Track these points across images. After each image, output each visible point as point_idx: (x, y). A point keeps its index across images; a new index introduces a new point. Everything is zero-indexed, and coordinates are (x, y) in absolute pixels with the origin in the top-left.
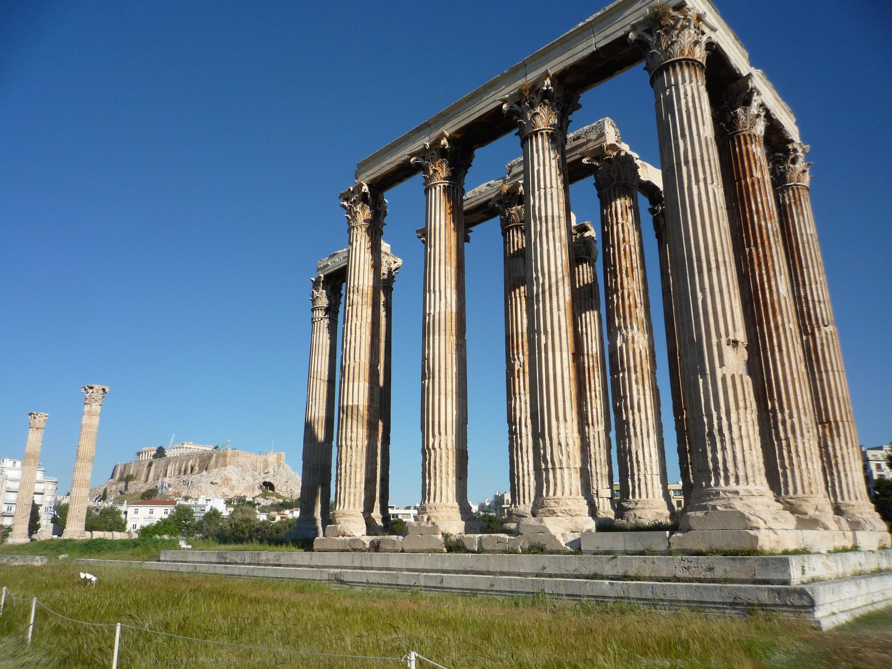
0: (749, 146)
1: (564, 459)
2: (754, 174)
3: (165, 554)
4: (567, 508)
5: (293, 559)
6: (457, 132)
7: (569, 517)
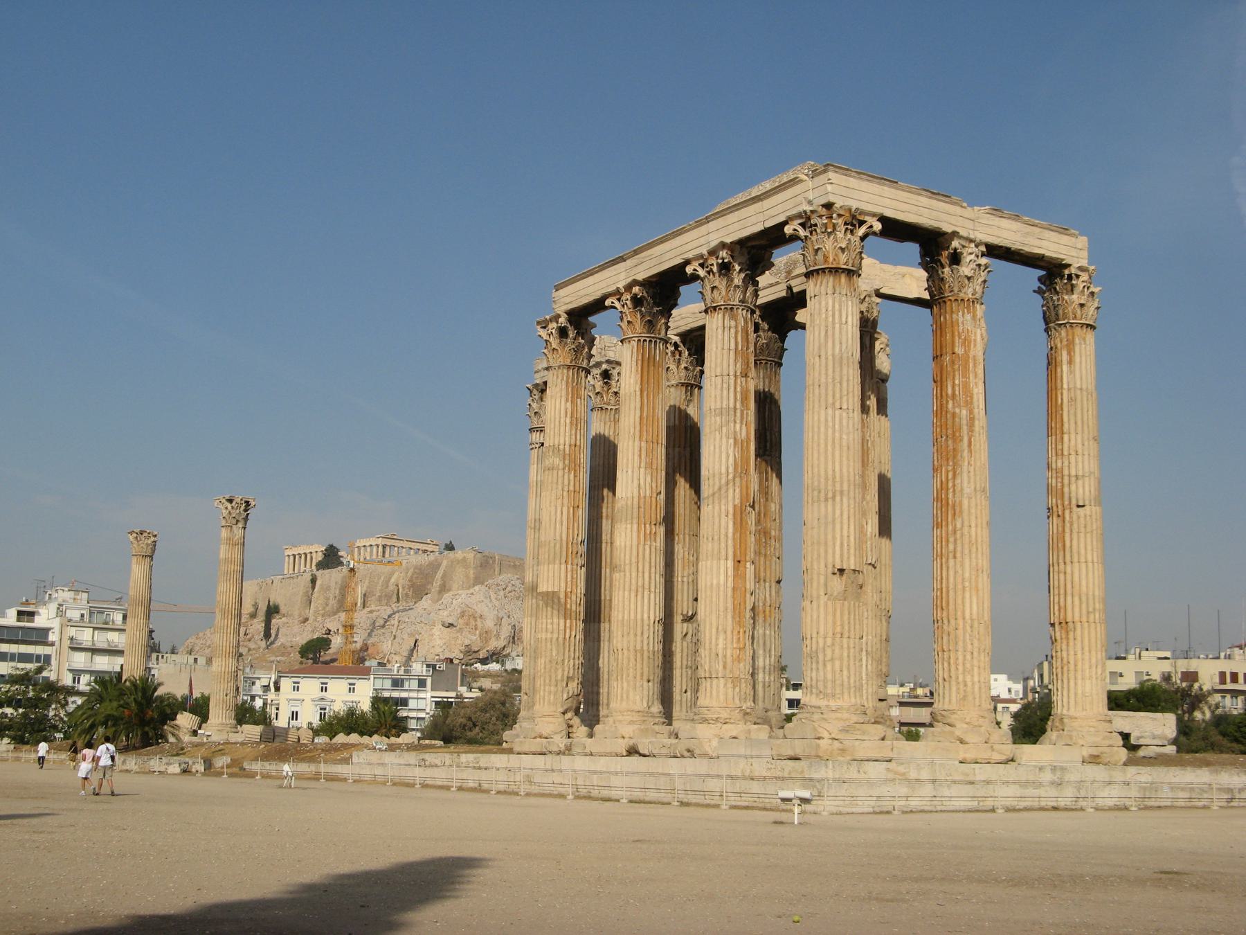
0: (954, 316)
1: (721, 668)
2: (956, 350)
4: (716, 716)
6: (651, 277)
7: (719, 725)
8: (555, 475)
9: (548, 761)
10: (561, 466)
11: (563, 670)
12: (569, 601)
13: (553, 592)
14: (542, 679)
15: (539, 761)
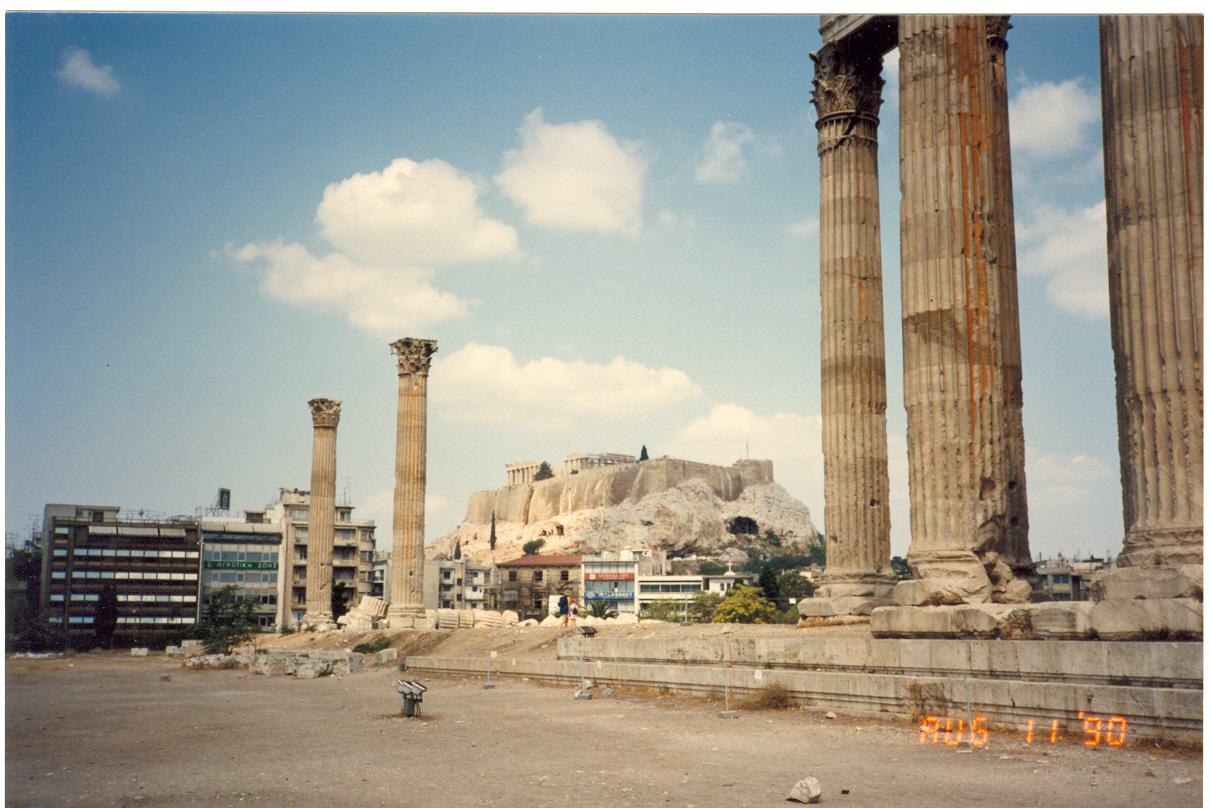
3: (566, 646)
5: (828, 654)
8: (930, 88)
9: (981, 654)
10: (941, 70)
11: (973, 466)
12: (975, 328)
13: (941, 311)
14: (928, 484)
15: (954, 654)
